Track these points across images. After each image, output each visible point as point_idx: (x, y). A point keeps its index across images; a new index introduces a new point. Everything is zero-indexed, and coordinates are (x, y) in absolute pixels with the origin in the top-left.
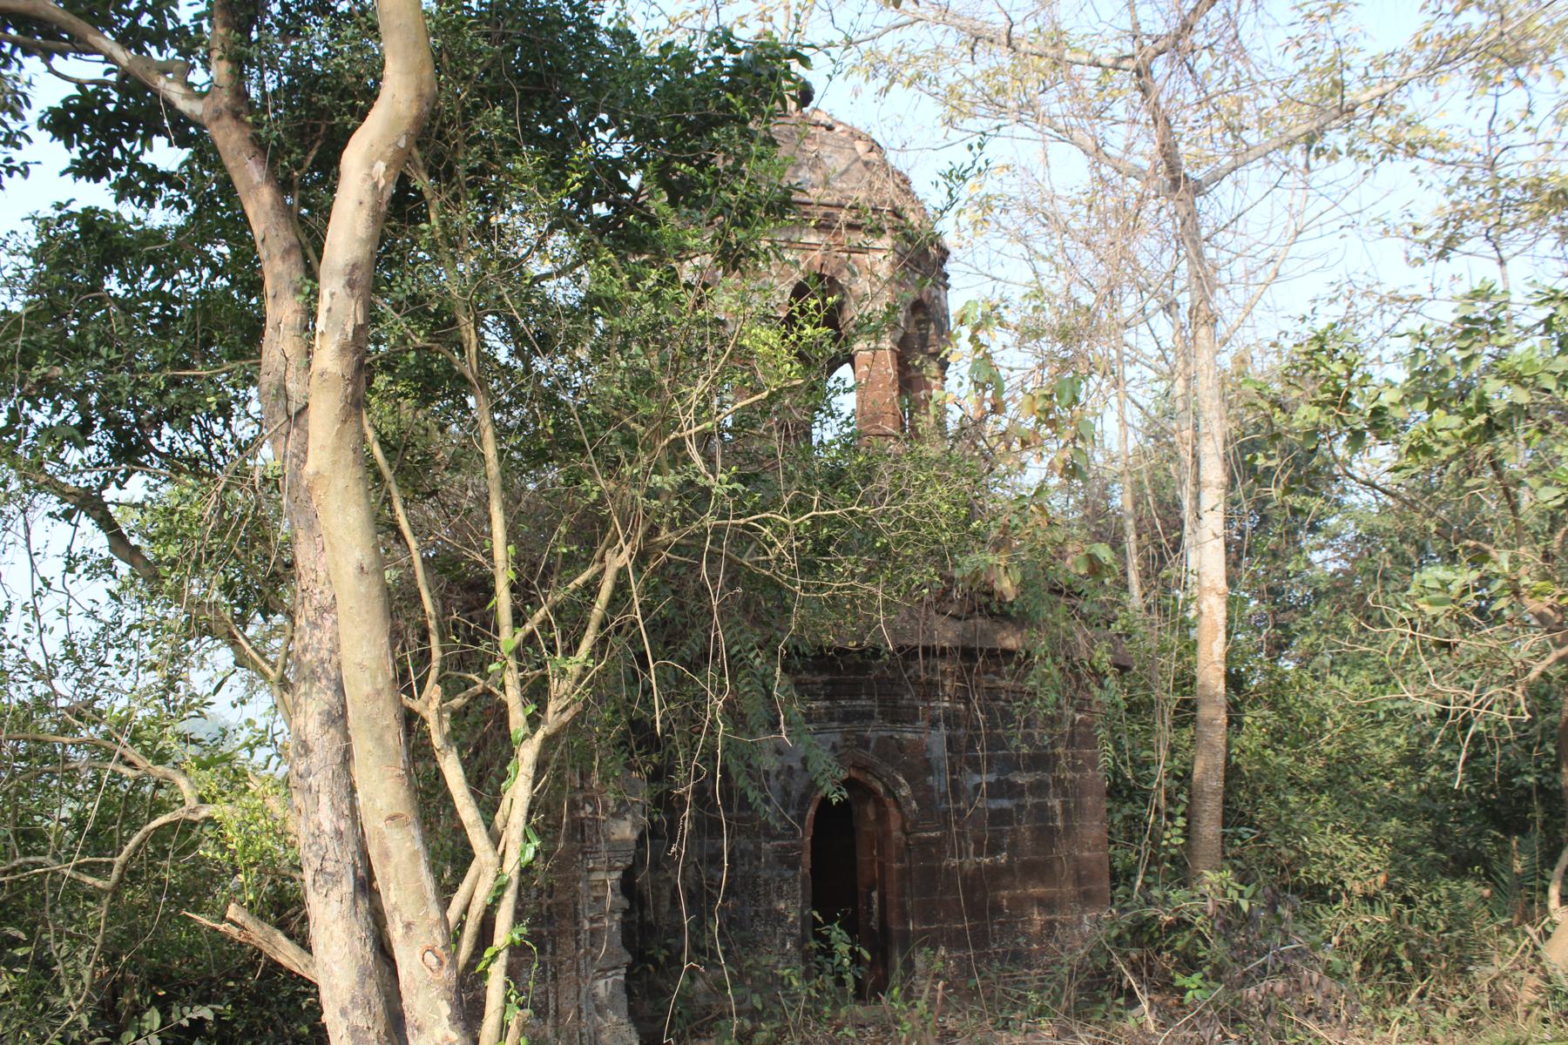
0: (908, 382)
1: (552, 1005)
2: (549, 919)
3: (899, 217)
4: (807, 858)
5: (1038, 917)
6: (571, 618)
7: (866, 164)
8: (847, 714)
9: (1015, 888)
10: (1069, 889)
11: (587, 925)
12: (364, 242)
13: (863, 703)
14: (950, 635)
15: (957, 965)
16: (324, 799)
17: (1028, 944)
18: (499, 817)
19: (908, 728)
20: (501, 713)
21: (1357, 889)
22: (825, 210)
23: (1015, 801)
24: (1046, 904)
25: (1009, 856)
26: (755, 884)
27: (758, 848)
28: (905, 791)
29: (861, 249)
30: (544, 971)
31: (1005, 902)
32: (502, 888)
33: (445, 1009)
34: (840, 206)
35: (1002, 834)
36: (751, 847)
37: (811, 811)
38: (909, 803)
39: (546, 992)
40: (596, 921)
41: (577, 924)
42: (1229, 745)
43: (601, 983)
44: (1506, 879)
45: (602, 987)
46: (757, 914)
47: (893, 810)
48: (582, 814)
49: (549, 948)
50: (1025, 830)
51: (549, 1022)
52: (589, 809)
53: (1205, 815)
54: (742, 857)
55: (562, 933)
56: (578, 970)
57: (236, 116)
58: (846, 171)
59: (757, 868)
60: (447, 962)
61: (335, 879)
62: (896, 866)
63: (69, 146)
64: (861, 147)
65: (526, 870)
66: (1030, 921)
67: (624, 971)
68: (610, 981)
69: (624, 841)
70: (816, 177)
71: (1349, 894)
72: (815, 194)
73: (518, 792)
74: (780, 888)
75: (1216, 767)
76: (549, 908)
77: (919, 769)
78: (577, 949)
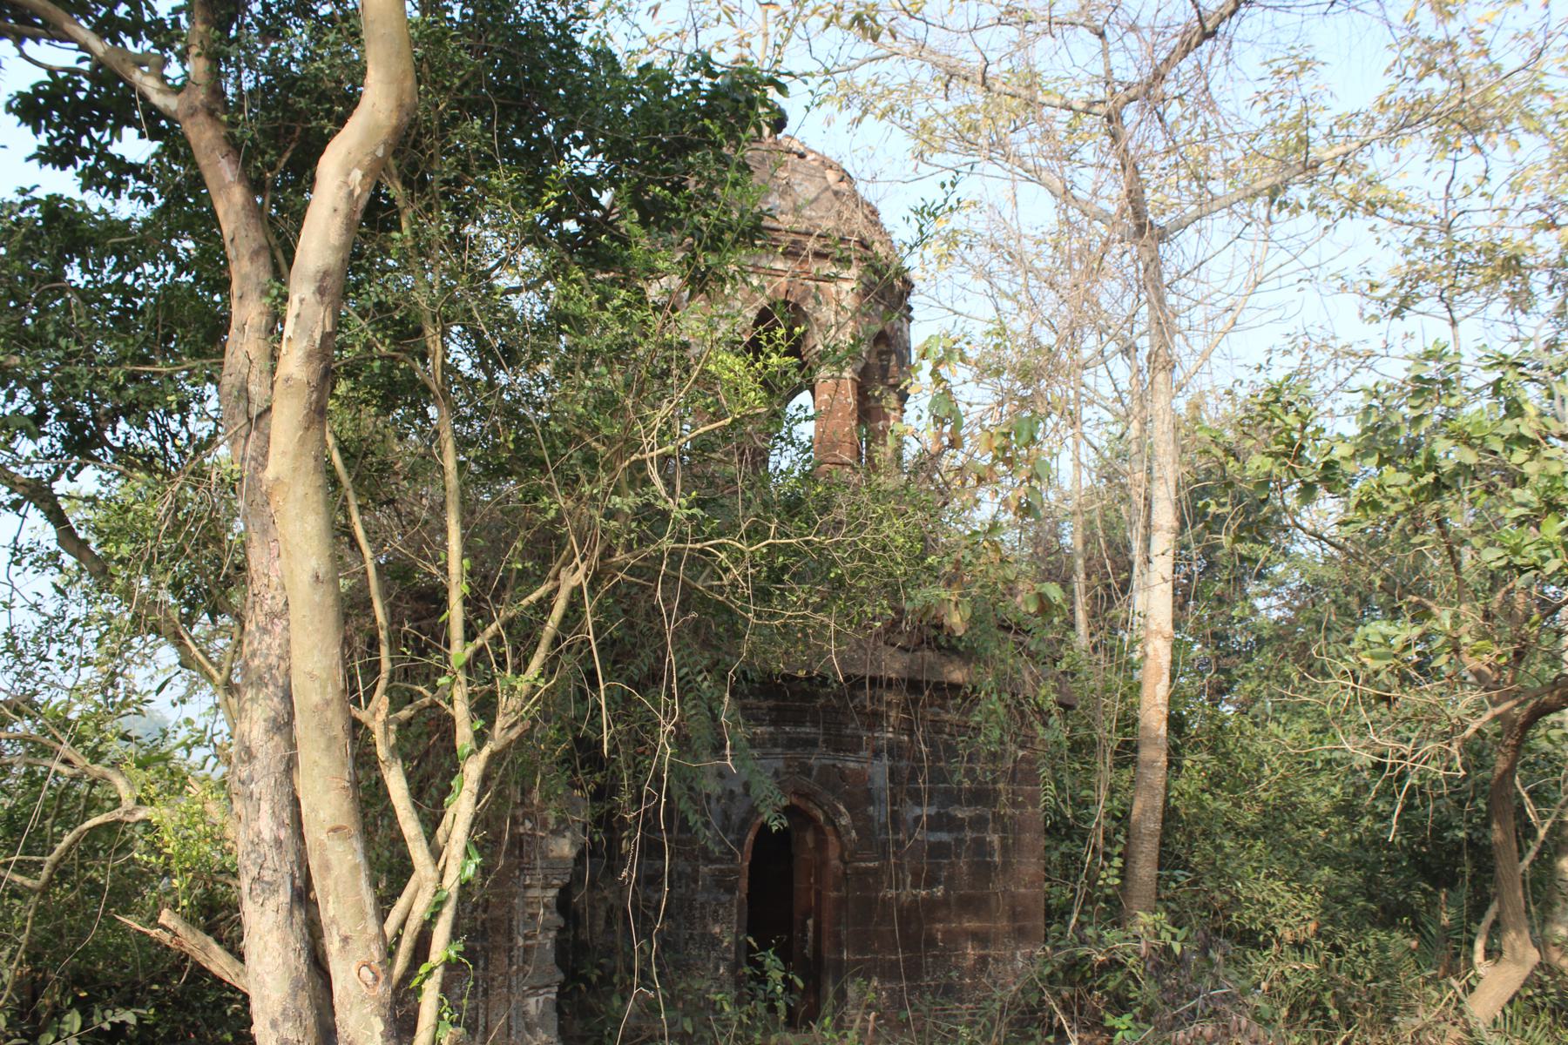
0: (867, 412)
1: (482, 1021)
3: (867, 248)
4: (744, 883)
5: (971, 952)
6: (523, 634)
7: (836, 193)
8: (791, 740)
10: (1003, 924)
11: (521, 942)
12: (337, 249)
13: (807, 730)
14: (897, 666)
15: (890, 996)
16: (265, 807)
17: (960, 978)
18: (441, 832)
19: (851, 756)
20: (446, 726)
21: (1288, 936)
22: (793, 237)
23: (954, 835)
24: (981, 939)
25: (946, 891)
26: (691, 907)
28: (845, 821)
29: (828, 279)
32: (440, 904)
33: (379, 1026)
34: (808, 234)
35: (940, 867)
37: (751, 837)
38: (848, 833)
41: (511, 940)
42: (1168, 788)
43: (532, 1001)
44: (1433, 931)
45: (533, 1005)
46: (691, 935)
47: (832, 839)
48: (521, 830)
49: (481, 963)
52: (528, 825)
53: (1142, 857)
54: (680, 879)
55: (495, 948)
56: (510, 987)
57: (211, 113)
58: (816, 199)
59: (694, 891)
60: (382, 978)
61: (272, 888)
62: (833, 894)
63: (36, 132)
64: (832, 176)
65: (465, 887)
66: (964, 955)
67: (556, 989)
68: (541, 999)
69: (562, 859)
70: (786, 204)
71: (1279, 941)
72: (786, 221)
73: (462, 808)
74: (716, 912)
75: (1154, 809)
76: (483, 923)
77: (860, 798)
78: (510, 965)
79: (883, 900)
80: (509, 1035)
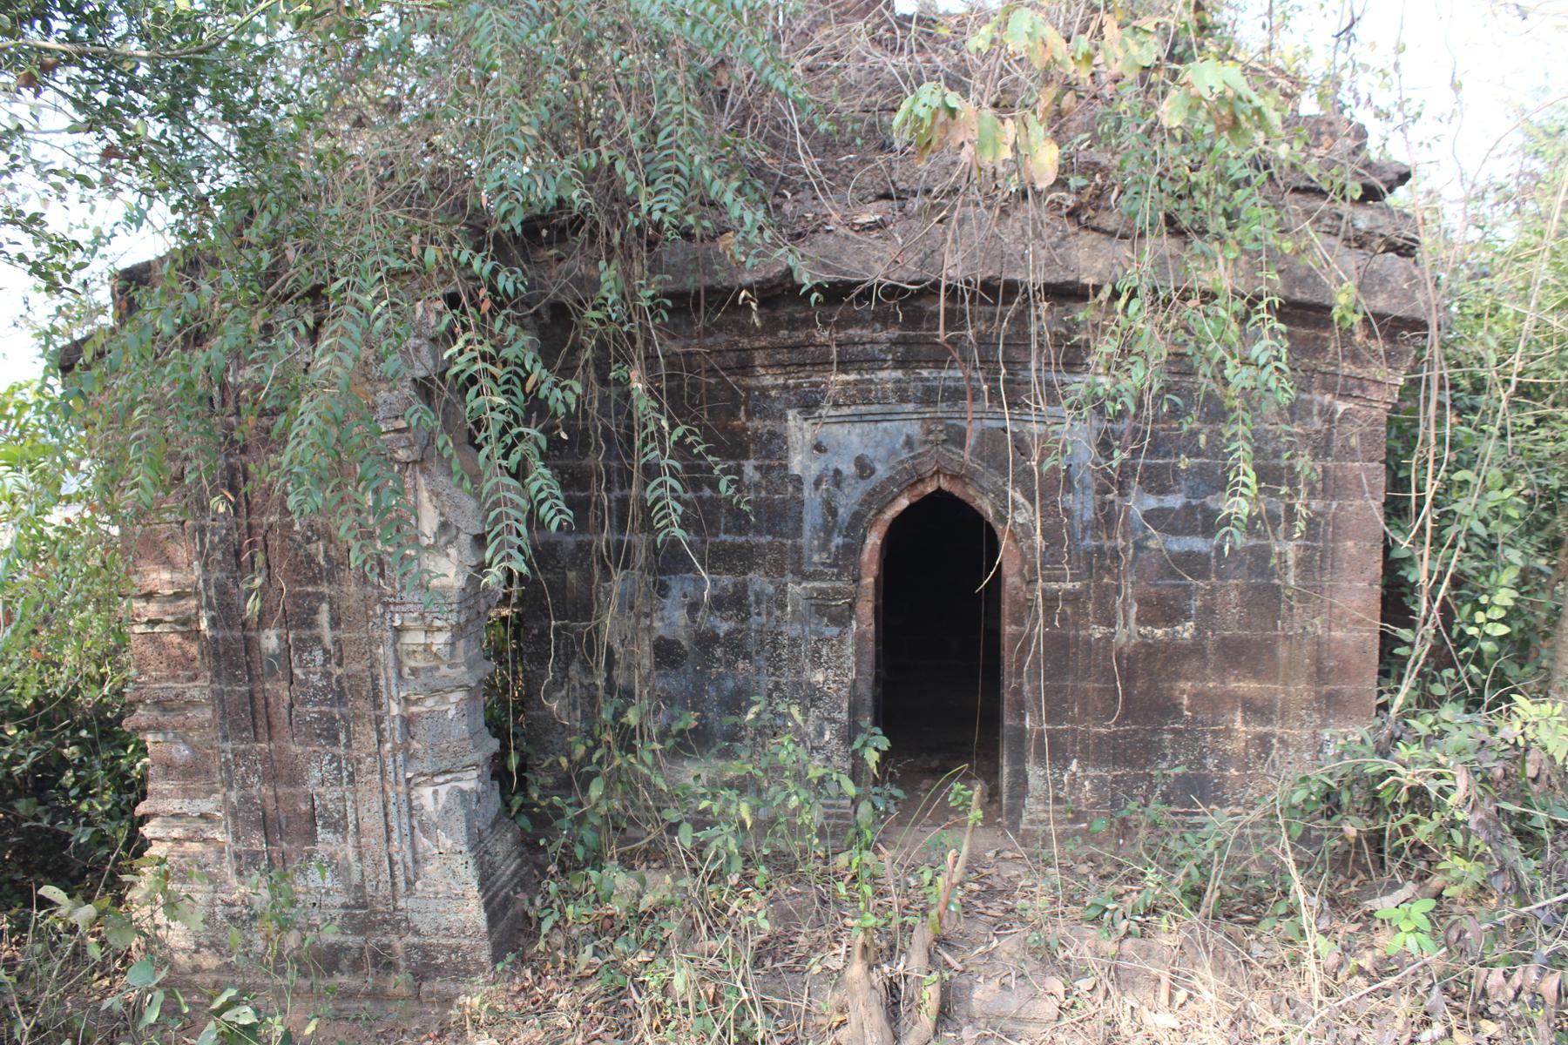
1: (351, 818)
2: (340, 697)
4: (866, 608)
5: (1242, 728)
9: (1205, 679)
11: (395, 709)
15: (1095, 789)
24: (1257, 710)
26: (775, 645)
27: (784, 592)
30: (339, 769)
31: (1185, 701)
35: (1188, 592)
36: (770, 589)
37: (874, 539)
39: (343, 799)
40: (415, 703)
43: (427, 792)
46: (777, 686)
49: (342, 736)
50: (1232, 592)
51: (350, 840)
54: (758, 602)
55: (358, 717)
56: (383, 773)
66: (1228, 733)
68: (443, 790)
74: (817, 651)
76: (339, 681)
79: (1087, 642)
80: (388, 840)
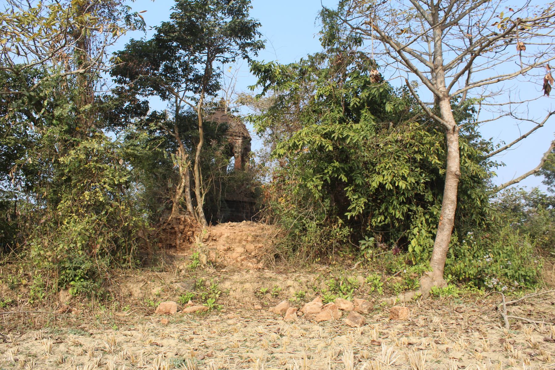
0: (243, 161)
6: (207, 184)
